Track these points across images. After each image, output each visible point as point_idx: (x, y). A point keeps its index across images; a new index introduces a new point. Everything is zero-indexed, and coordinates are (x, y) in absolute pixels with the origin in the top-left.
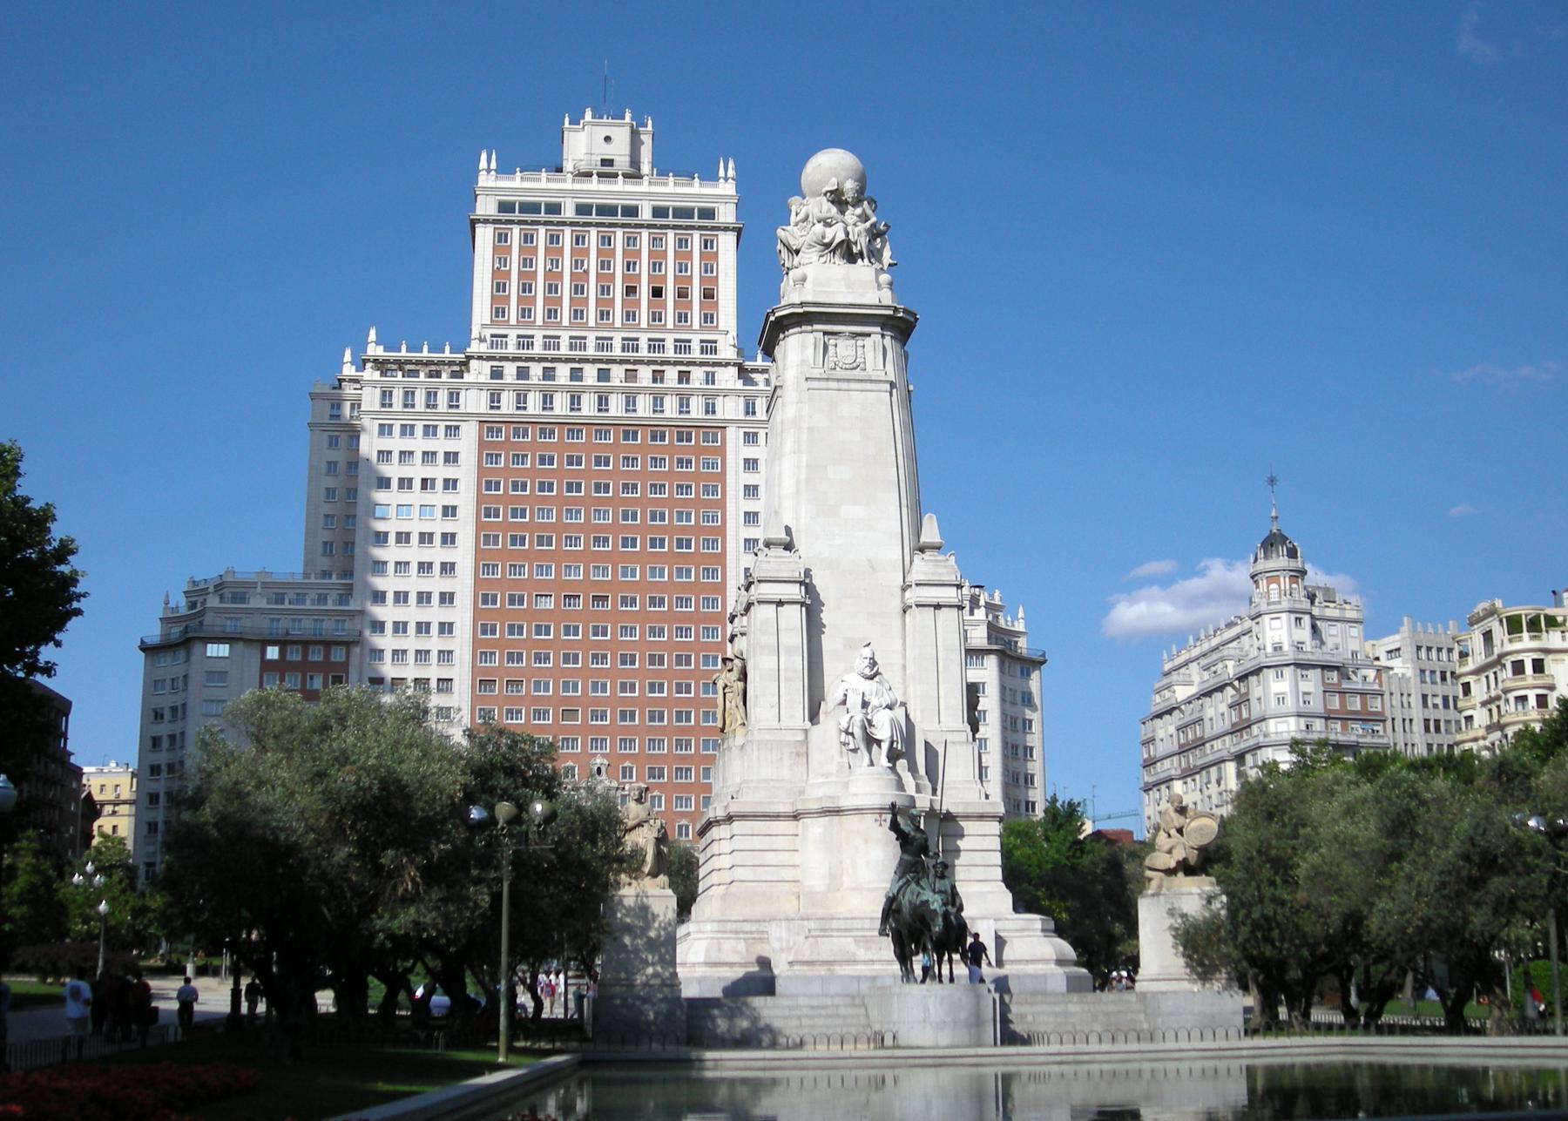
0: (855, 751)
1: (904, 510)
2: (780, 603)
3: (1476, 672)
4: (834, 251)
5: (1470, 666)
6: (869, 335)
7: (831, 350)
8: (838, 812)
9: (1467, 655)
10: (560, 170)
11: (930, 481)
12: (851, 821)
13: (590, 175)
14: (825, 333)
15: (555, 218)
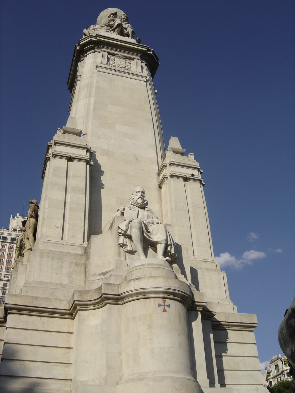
0: (132, 252)
1: (157, 136)
2: (70, 159)
3: (274, 377)
4: (114, 30)
5: (271, 376)
6: (133, 59)
7: (112, 61)
8: (118, 299)
9: (270, 373)
10: (8, 229)
11: (174, 120)
12: (133, 308)
13: (16, 230)
14: (109, 53)
15: (5, 241)
